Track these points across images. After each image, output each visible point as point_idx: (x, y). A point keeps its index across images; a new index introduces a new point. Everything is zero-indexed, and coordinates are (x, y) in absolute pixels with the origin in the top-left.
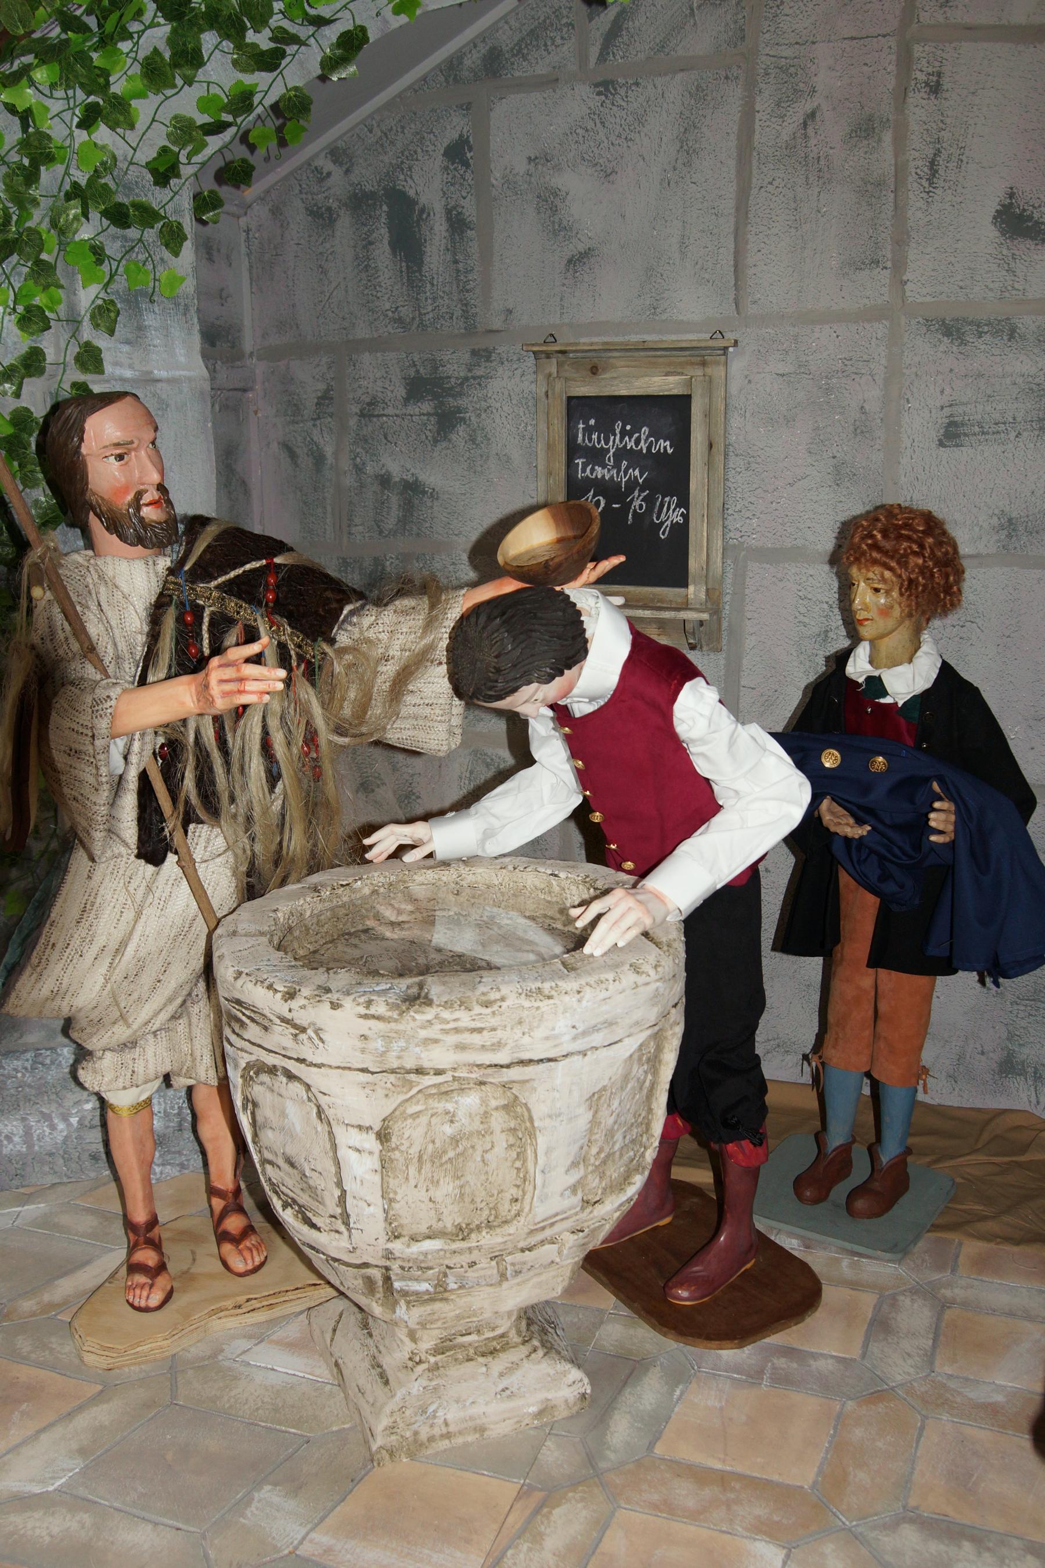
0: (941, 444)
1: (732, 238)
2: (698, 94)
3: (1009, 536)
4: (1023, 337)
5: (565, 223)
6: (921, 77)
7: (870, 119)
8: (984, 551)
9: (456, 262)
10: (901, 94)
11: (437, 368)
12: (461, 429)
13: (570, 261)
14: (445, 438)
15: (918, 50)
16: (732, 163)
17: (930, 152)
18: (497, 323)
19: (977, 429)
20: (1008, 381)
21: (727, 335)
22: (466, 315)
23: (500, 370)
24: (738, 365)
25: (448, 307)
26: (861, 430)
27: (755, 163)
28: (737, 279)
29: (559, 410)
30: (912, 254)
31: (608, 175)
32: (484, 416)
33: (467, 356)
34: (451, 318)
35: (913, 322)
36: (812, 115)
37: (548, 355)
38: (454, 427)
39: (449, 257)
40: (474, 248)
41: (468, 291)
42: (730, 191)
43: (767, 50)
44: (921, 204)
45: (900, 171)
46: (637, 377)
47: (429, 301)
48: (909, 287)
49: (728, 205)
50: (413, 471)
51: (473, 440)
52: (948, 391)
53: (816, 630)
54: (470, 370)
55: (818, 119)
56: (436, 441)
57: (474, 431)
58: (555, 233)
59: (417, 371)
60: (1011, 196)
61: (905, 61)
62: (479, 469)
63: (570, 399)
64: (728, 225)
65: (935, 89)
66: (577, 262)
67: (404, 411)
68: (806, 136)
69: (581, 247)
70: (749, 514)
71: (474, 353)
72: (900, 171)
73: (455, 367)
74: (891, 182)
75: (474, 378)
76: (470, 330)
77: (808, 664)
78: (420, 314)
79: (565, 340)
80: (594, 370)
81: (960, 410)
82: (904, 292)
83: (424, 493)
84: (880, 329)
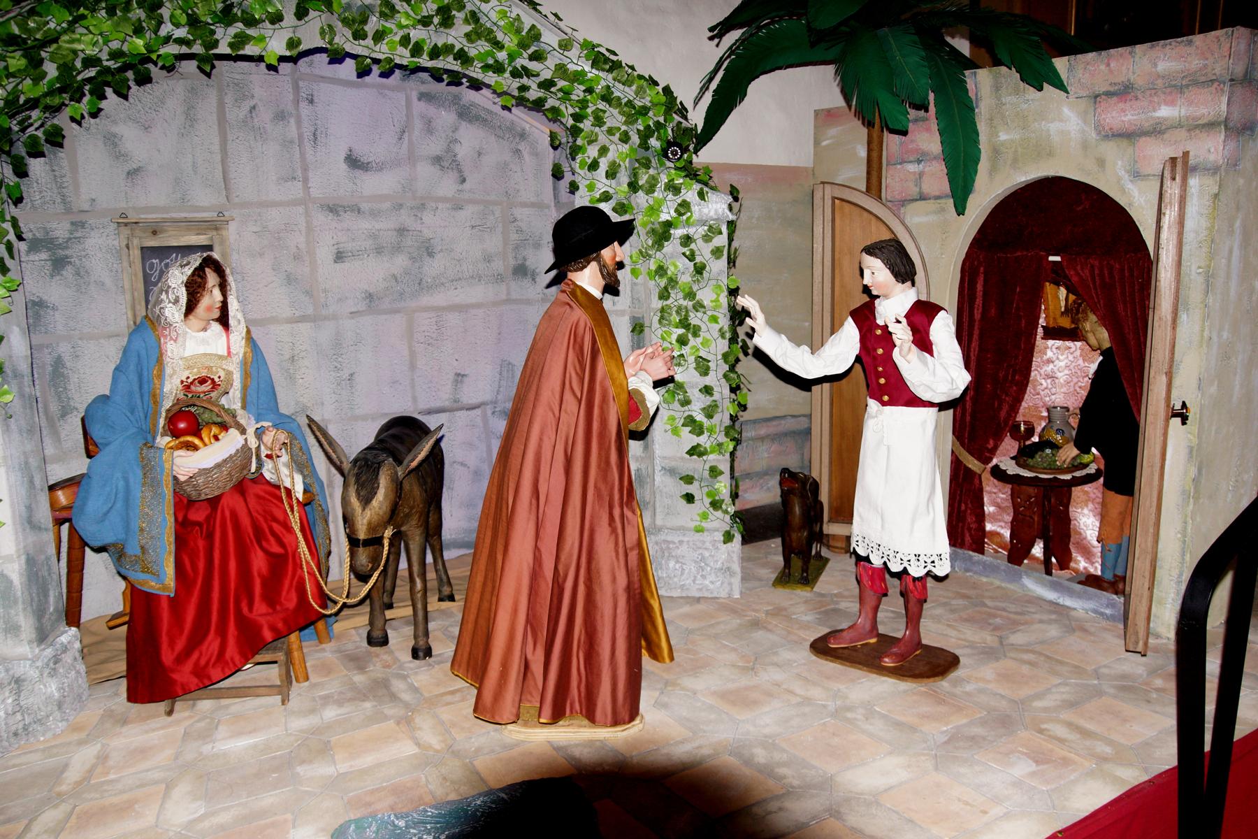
0: (335, 262)
1: (220, 164)
2: (193, 91)
3: (370, 301)
4: (363, 212)
5: (123, 152)
6: (305, 96)
7: (283, 112)
8: (361, 309)
9: (54, 171)
10: (297, 102)
11: (48, 233)
12: (69, 268)
13: (128, 173)
14: (58, 274)
15: (301, 84)
16: (216, 127)
17: (313, 129)
18: (86, 207)
19: (350, 254)
20: (361, 232)
21: (225, 213)
22: (64, 201)
23: (92, 233)
24: (232, 227)
25: (51, 196)
26: (297, 257)
27: (228, 129)
28: (225, 185)
29: (136, 253)
30: (310, 174)
31: (147, 128)
32: (84, 260)
33: (68, 225)
34: (54, 203)
35: (315, 206)
36: (254, 107)
37: (126, 224)
38: (64, 267)
39: (48, 167)
40: (65, 163)
41: (63, 188)
42: (216, 140)
43: (227, 75)
44: (312, 152)
45: (300, 136)
46: (182, 236)
47: (37, 193)
48: (311, 190)
49: (216, 148)
50: (37, 294)
51: (78, 274)
52: (335, 237)
53: (288, 357)
54: (72, 234)
55: (257, 109)
56: (52, 276)
57: (78, 269)
58: (117, 158)
59: (34, 235)
60: (350, 151)
61: (296, 88)
62: (84, 290)
63: (142, 248)
64: (218, 158)
65: (311, 102)
66: (132, 174)
67: (27, 259)
68: (252, 117)
69: (135, 166)
70: (247, 303)
71: (72, 224)
72: (300, 136)
73: (61, 232)
74: (297, 141)
75: (75, 238)
76: (69, 211)
77: (286, 374)
78: (31, 200)
79: (133, 217)
80: (154, 233)
81: (342, 245)
82: (309, 192)
83: (47, 307)
84: (301, 209)
